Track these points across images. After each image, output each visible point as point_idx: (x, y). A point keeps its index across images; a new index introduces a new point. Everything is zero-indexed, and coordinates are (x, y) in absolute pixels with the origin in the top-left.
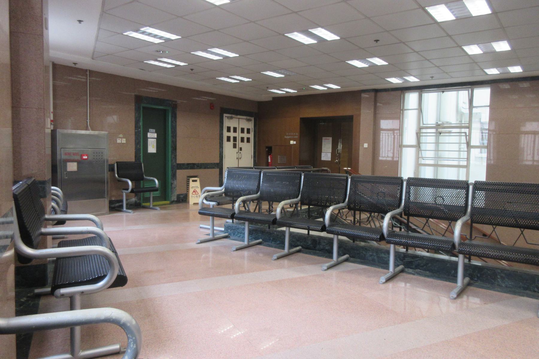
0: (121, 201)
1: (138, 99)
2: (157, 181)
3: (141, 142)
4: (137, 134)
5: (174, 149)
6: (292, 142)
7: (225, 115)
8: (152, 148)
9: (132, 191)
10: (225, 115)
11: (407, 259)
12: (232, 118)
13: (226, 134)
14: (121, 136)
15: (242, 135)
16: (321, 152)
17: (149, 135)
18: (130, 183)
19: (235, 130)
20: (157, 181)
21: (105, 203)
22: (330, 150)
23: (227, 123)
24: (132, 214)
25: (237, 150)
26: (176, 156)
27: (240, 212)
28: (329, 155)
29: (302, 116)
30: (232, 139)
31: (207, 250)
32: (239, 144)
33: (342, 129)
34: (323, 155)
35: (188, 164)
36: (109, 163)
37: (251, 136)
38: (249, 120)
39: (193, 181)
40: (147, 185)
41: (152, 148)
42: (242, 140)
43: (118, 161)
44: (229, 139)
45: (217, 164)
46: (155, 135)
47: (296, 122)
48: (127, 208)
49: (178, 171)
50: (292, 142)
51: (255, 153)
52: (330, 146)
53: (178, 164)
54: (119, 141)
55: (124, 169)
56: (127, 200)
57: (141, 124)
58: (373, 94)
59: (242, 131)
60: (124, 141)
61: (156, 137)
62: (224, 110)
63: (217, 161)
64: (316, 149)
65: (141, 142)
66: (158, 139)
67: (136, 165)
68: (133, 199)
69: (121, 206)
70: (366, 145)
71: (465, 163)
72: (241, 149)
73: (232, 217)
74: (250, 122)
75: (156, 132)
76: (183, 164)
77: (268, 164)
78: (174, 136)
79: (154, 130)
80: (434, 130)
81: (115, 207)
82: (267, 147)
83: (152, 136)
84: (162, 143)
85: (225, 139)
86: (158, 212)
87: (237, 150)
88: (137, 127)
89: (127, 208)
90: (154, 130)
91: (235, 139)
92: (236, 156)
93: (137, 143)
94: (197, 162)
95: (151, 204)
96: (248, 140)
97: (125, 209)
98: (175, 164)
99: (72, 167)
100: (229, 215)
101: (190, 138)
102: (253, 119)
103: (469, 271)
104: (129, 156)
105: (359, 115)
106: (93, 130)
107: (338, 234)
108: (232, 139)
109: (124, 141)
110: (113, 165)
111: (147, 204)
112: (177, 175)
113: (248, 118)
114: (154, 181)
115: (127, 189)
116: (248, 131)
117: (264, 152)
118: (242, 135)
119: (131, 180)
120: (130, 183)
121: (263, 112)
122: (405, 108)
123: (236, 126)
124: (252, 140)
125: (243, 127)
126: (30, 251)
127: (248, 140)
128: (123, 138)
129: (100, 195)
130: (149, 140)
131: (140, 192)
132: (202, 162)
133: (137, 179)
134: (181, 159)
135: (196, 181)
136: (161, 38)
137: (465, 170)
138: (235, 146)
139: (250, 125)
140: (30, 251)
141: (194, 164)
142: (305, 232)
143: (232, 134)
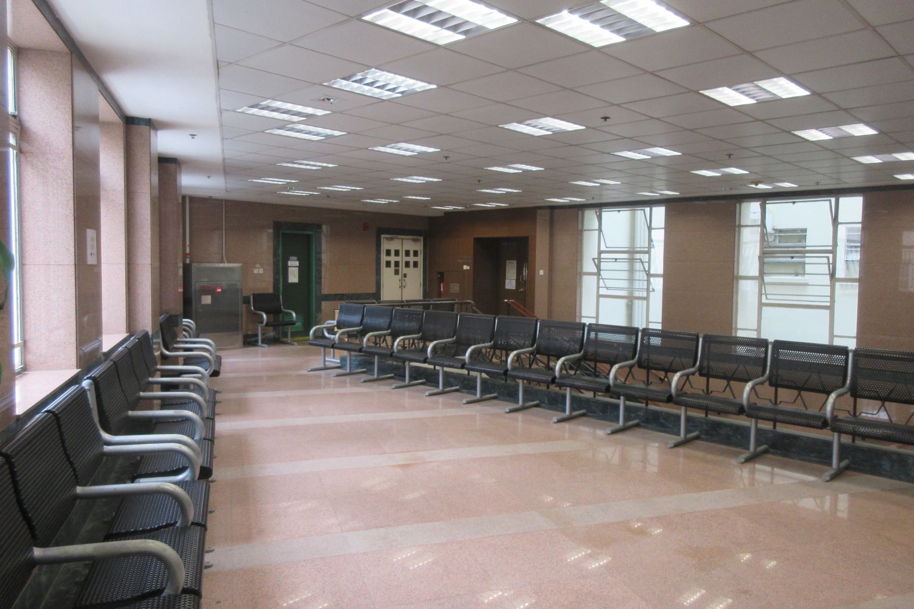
0: (257, 335)
1: (277, 226)
2: (294, 315)
3: (281, 271)
4: (276, 264)
5: (319, 278)
6: (465, 267)
7: (383, 236)
8: (293, 277)
9: (267, 325)
10: (383, 236)
11: (466, 382)
12: (392, 239)
13: (384, 258)
14: (258, 266)
15: (398, 259)
16: (505, 279)
17: (290, 263)
18: (265, 316)
19: (397, 253)
20: (294, 315)
21: (240, 338)
22: (515, 277)
23: (385, 245)
24: (266, 348)
25: (399, 277)
27: (368, 347)
28: (514, 282)
29: (476, 236)
30: (393, 264)
31: (319, 377)
32: (403, 269)
33: (521, 250)
34: (507, 282)
35: (335, 295)
36: (245, 294)
37: (420, 259)
38: (415, 240)
40: (287, 319)
41: (293, 277)
42: (407, 264)
44: (388, 264)
45: (373, 294)
46: (297, 263)
47: (470, 243)
48: (263, 342)
49: (323, 303)
50: (465, 267)
51: (424, 279)
52: (515, 271)
54: (256, 271)
55: (262, 301)
56: (263, 334)
57: (280, 252)
58: (548, 211)
59: (407, 253)
60: (261, 271)
62: (381, 231)
63: (373, 290)
64: (500, 277)
65: (281, 271)
66: (300, 267)
67: (274, 297)
68: (271, 334)
69: (257, 341)
70: (541, 272)
71: (645, 295)
72: (405, 276)
73: (360, 350)
74: (418, 243)
75: (298, 260)
76: (330, 295)
77: (440, 295)
80: (625, 256)
81: (249, 341)
82: (439, 273)
83: (294, 265)
84: (305, 271)
85: (383, 264)
86: (297, 347)
87: (399, 277)
88: (275, 255)
89: (263, 342)
91: (397, 264)
92: (399, 284)
93: (276, 273)
95: (289, 340)
96: (416, 264)
97: (260, 343)
99: (207, 300)
100: (460, 365)
101: (335, 266)
102: (422, 238)
103: (577, 403)
104: (266, 286)
105: (535, 237)
106: (229, 262)
107: (443, 366)
108: (393, 264)
109: (261, 271)
110: (249, 297)
111: (285, 339)
112: (323, 308)
113: (415, 237)
114: (291, 314)
115: (262, 323)
117: (434, 278)
118: (398, 259)
119: (266, 313)
120: (265, 316)
121: (432, 230)
122: (585, 228)
123: (399, 247)
124: (421, 264)
126: (167, 353)
127: (416, 264)
129: (234, 328)
130: (290, 269)
131: (279, 325)
132: (353, 292)
133: (274, 312)
134: (325, 290)
136: (318, 134)
137: (645, 302)
138: (397, 272)
139: (419, 247)
140: (167, 353)
141: (343, 295)
142: (432, 367)
143: (393, 259)
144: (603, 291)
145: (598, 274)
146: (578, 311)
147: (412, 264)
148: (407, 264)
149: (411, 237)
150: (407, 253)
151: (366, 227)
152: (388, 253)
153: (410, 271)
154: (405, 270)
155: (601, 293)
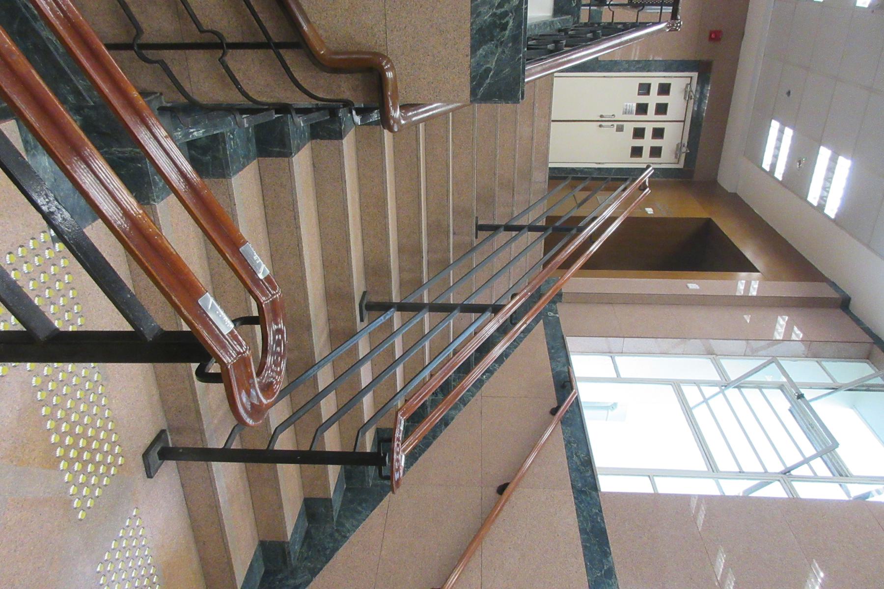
7: (695, 75)
10: (695, 75)
13: (655, 79)
19: (662, 109)
23: (679, 81)
38: (679, 147)
44: (645, 89)
72: (620, 129)
74: (673, 159)
96: (637, 152)
102: (681, 166)
116: (656, 152)
125: (666, 134)
145: (726, 384)
146: (630, 343)
147: (638, 143)
148: (639, 133)
149: (685, 141)
150: (658, 133)
151: (715, 36)
152: (664, 89)
153: (627, 141)
154: (629, 128)
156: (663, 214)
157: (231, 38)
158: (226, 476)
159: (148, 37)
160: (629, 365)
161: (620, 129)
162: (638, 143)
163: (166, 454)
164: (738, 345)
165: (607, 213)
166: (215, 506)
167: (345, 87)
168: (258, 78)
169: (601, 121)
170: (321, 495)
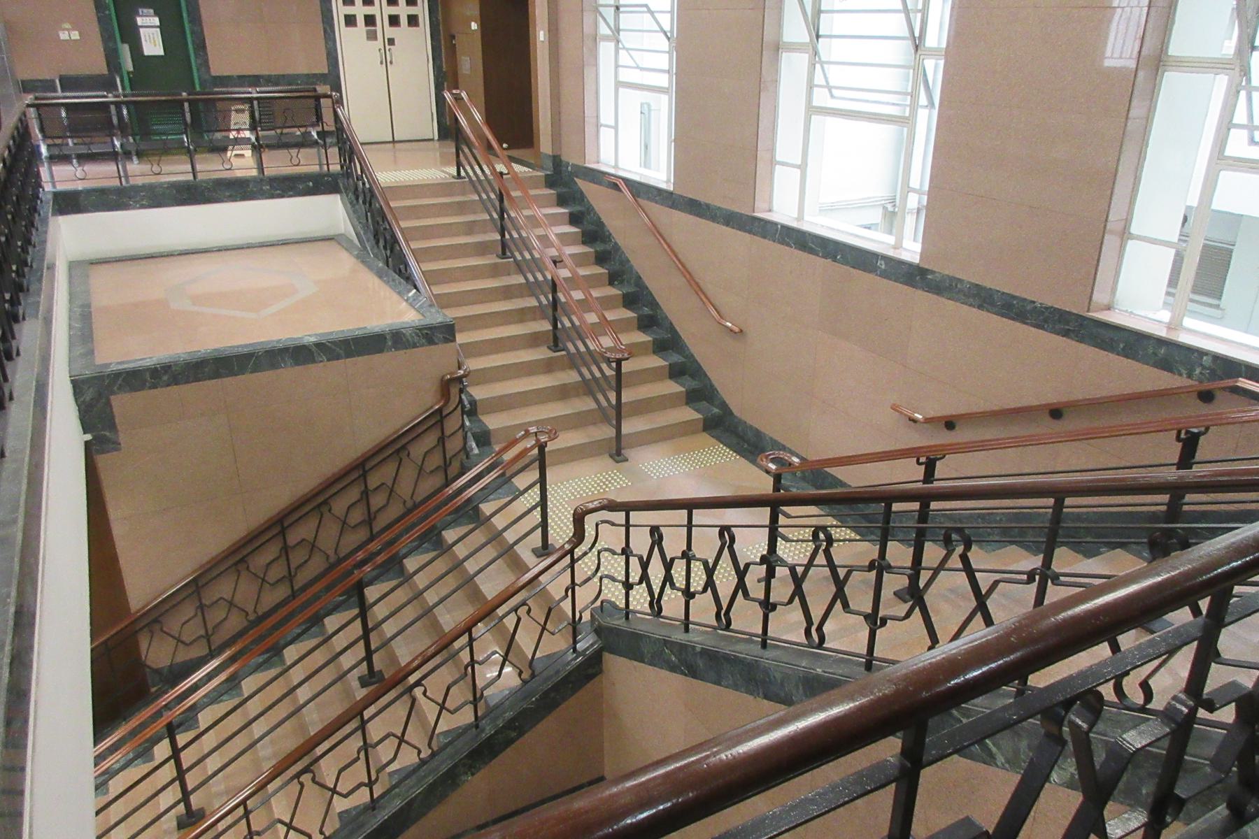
5: (201, 46)
17: (140, 21)
26: (206, 61)
30: (360, 21)
35: (240, 77)
39: (237, 111)
41: (152, 44)
43: (63, 73)
44: (350, 21)
46: (156, 21)
53: (215, 78)
54: (64, 36)
60: (75, 35)
61: (158, 23)
72: (391, 42)
75: (156, 14)
78: (196, 19)
79: (152, 11)
85: (339, 21)
90: (152, 11)
91: (370, 20)
94: (267, 73)
96: (413, 21)
98: (207, 77)
110: (53, 81)
127: (413, 21)
128: (74, 29)
135: (242, 111)
138: (372, 36)
144: (625, 76)
147: (404, 21)
148: (394, 21)
153: (402, 32)
154: (391, 32)
155: (621, 79)
156: (476, 12)
157: (440, 434)
158: (628, 427)
159: (442, 463)
160: (606, 116)
161: (391, 42)
162: (404, 21)
163: (619, 453)
164: (588, 19)
165: (485, 167)
166: (651, 431)
167: (454, 391)
168: (451, 424)
169: (386, 62)
170: (667, 370)
